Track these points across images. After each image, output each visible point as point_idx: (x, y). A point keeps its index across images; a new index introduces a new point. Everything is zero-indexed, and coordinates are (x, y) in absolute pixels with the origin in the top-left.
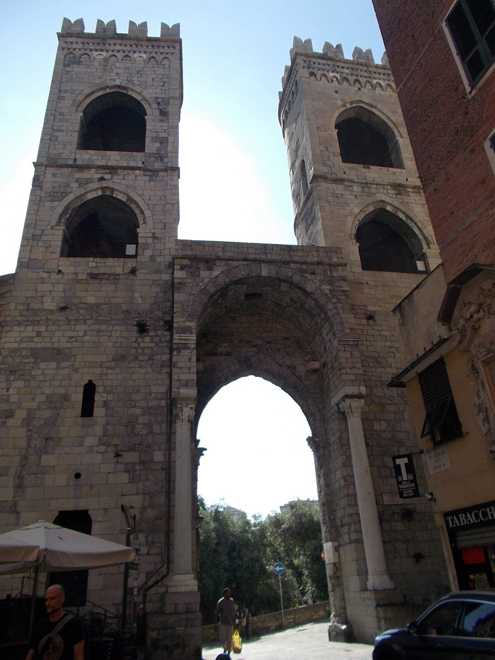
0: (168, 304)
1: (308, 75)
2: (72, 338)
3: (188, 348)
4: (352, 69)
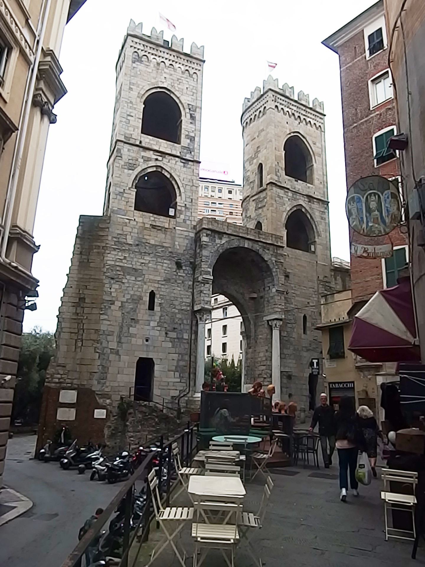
0: (192, 252)
1: (274, 107)
2: (143, 263)
3: (208, 283)
4: (298, 107)
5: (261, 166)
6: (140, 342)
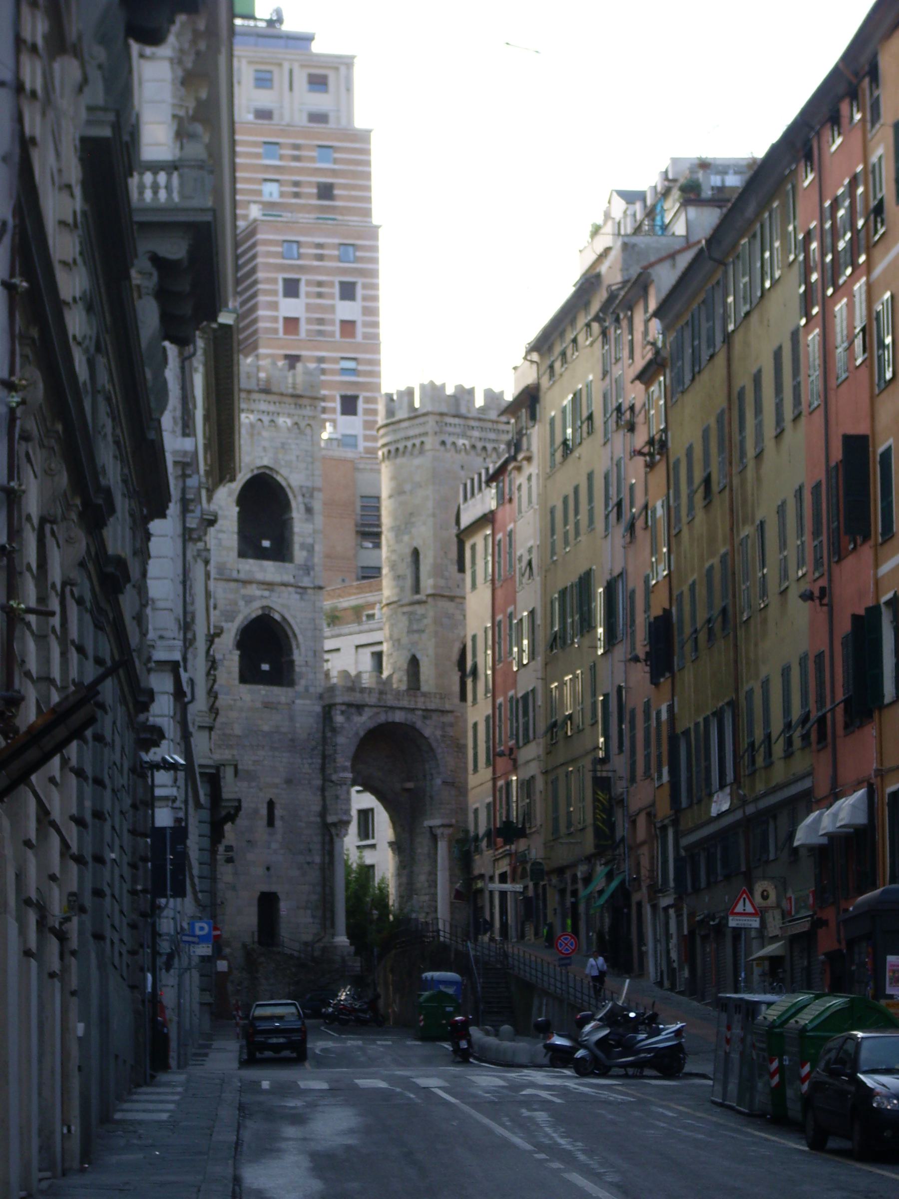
0: (320, 735)
1: (438, 446)
5: (416, 553)
6: (260, 871)
